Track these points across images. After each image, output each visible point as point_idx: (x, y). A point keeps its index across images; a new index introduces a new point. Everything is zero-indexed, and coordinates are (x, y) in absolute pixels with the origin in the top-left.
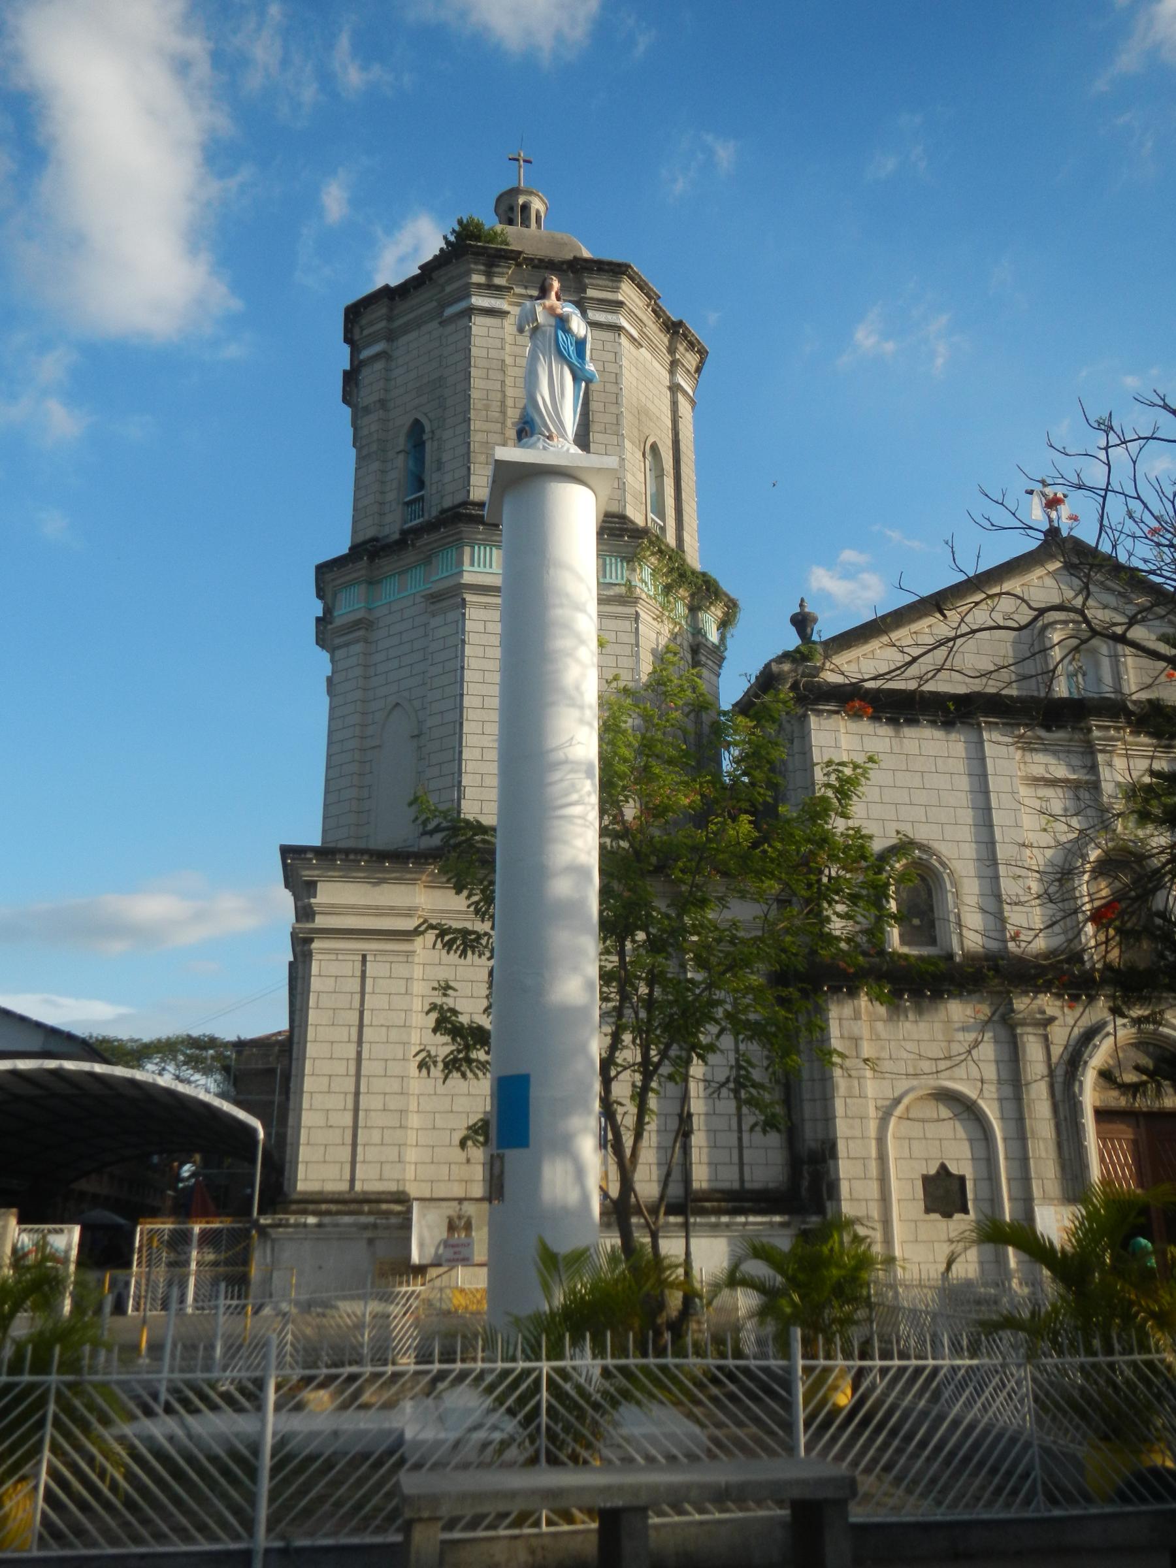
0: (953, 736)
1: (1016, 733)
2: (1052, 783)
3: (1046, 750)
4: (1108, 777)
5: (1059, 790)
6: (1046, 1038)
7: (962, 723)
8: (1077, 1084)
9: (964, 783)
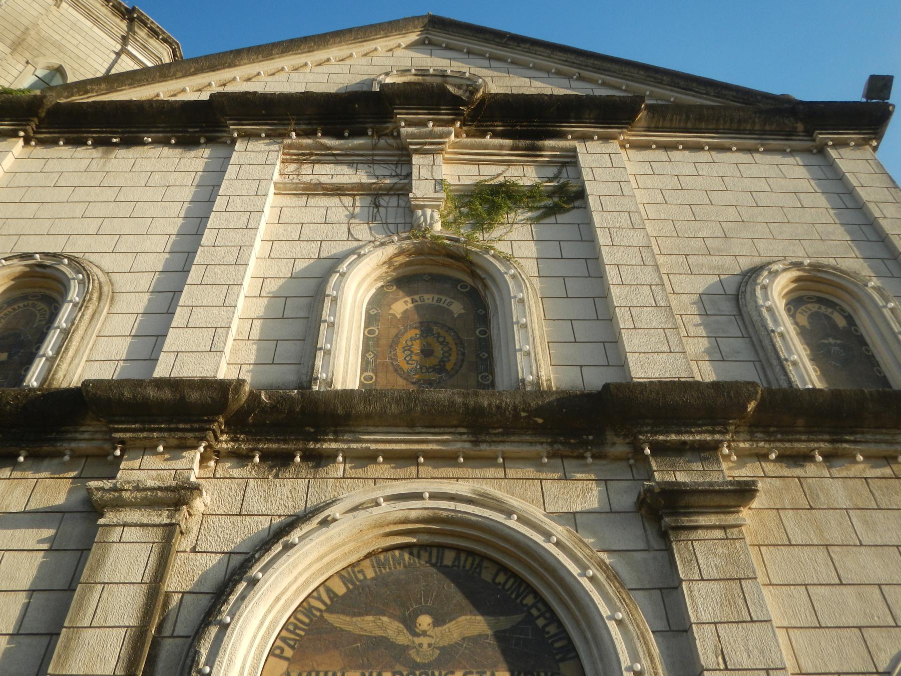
0: (193, 153)
1: (287, 141)
2: (336, 191)
3: (337, 163)
4: (424, 173)
5: (348, 201)
6: (170, 531)
7: (210, 141)
8: (213, 630)
9: (188, 194)
